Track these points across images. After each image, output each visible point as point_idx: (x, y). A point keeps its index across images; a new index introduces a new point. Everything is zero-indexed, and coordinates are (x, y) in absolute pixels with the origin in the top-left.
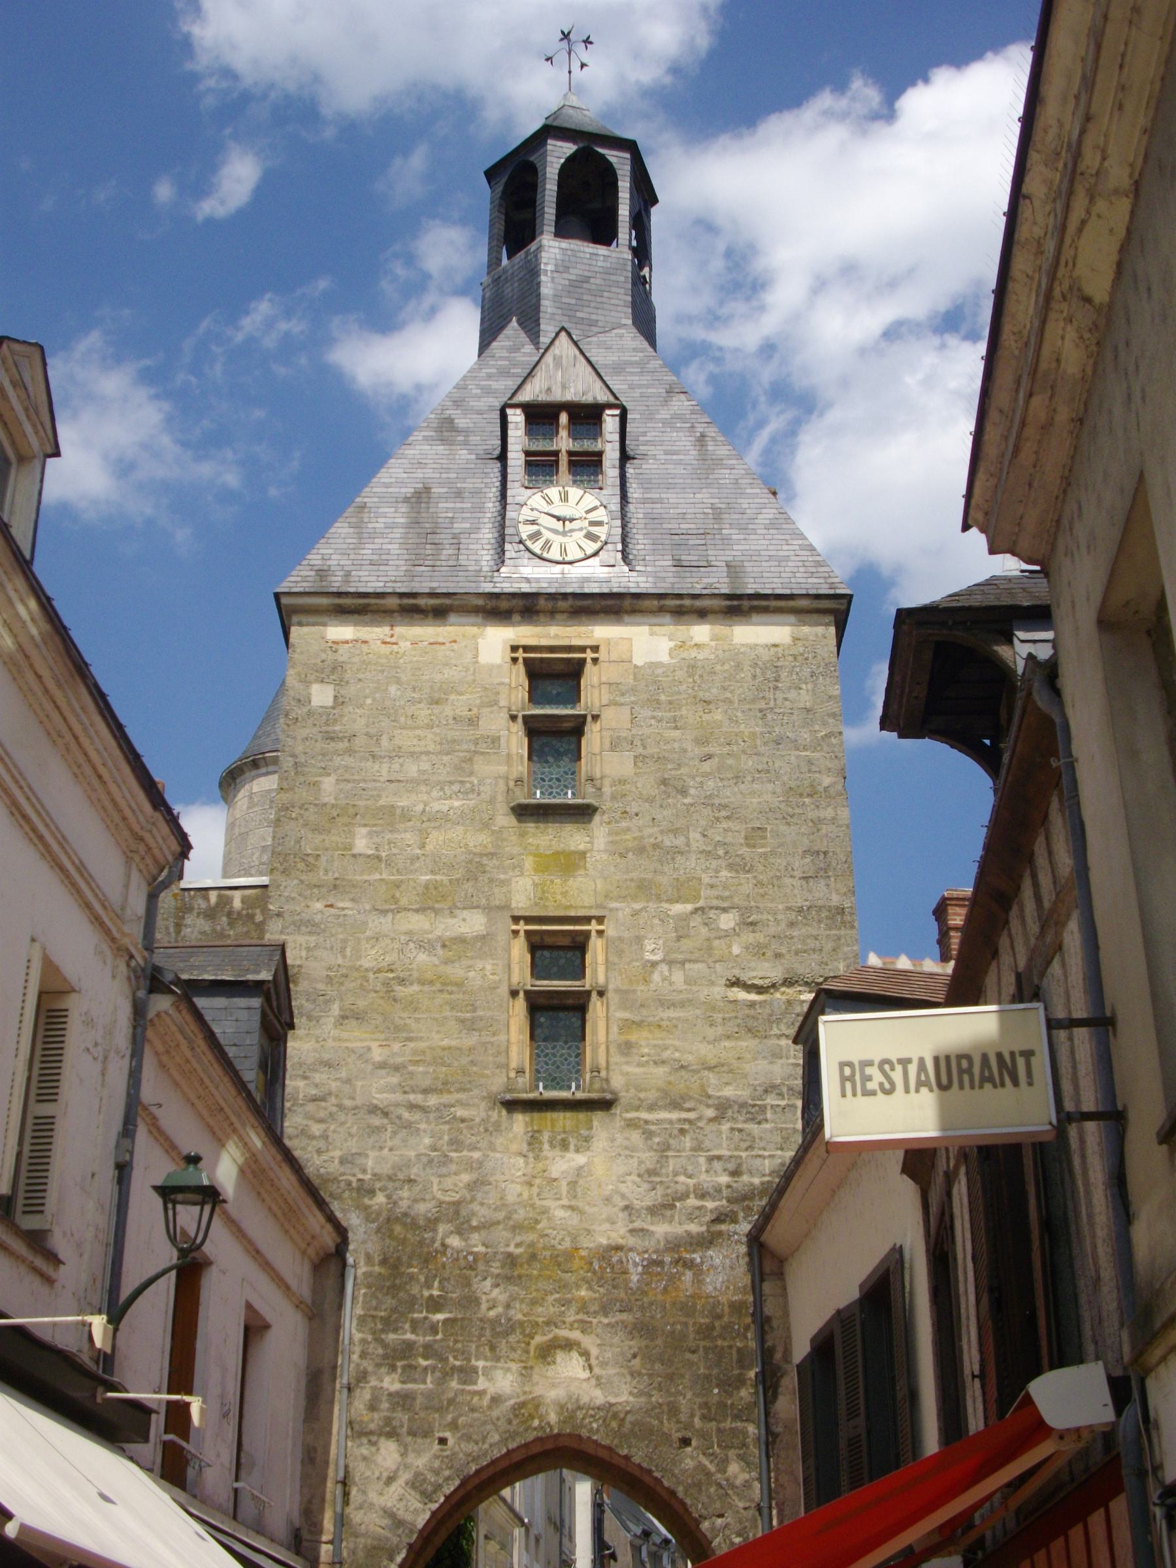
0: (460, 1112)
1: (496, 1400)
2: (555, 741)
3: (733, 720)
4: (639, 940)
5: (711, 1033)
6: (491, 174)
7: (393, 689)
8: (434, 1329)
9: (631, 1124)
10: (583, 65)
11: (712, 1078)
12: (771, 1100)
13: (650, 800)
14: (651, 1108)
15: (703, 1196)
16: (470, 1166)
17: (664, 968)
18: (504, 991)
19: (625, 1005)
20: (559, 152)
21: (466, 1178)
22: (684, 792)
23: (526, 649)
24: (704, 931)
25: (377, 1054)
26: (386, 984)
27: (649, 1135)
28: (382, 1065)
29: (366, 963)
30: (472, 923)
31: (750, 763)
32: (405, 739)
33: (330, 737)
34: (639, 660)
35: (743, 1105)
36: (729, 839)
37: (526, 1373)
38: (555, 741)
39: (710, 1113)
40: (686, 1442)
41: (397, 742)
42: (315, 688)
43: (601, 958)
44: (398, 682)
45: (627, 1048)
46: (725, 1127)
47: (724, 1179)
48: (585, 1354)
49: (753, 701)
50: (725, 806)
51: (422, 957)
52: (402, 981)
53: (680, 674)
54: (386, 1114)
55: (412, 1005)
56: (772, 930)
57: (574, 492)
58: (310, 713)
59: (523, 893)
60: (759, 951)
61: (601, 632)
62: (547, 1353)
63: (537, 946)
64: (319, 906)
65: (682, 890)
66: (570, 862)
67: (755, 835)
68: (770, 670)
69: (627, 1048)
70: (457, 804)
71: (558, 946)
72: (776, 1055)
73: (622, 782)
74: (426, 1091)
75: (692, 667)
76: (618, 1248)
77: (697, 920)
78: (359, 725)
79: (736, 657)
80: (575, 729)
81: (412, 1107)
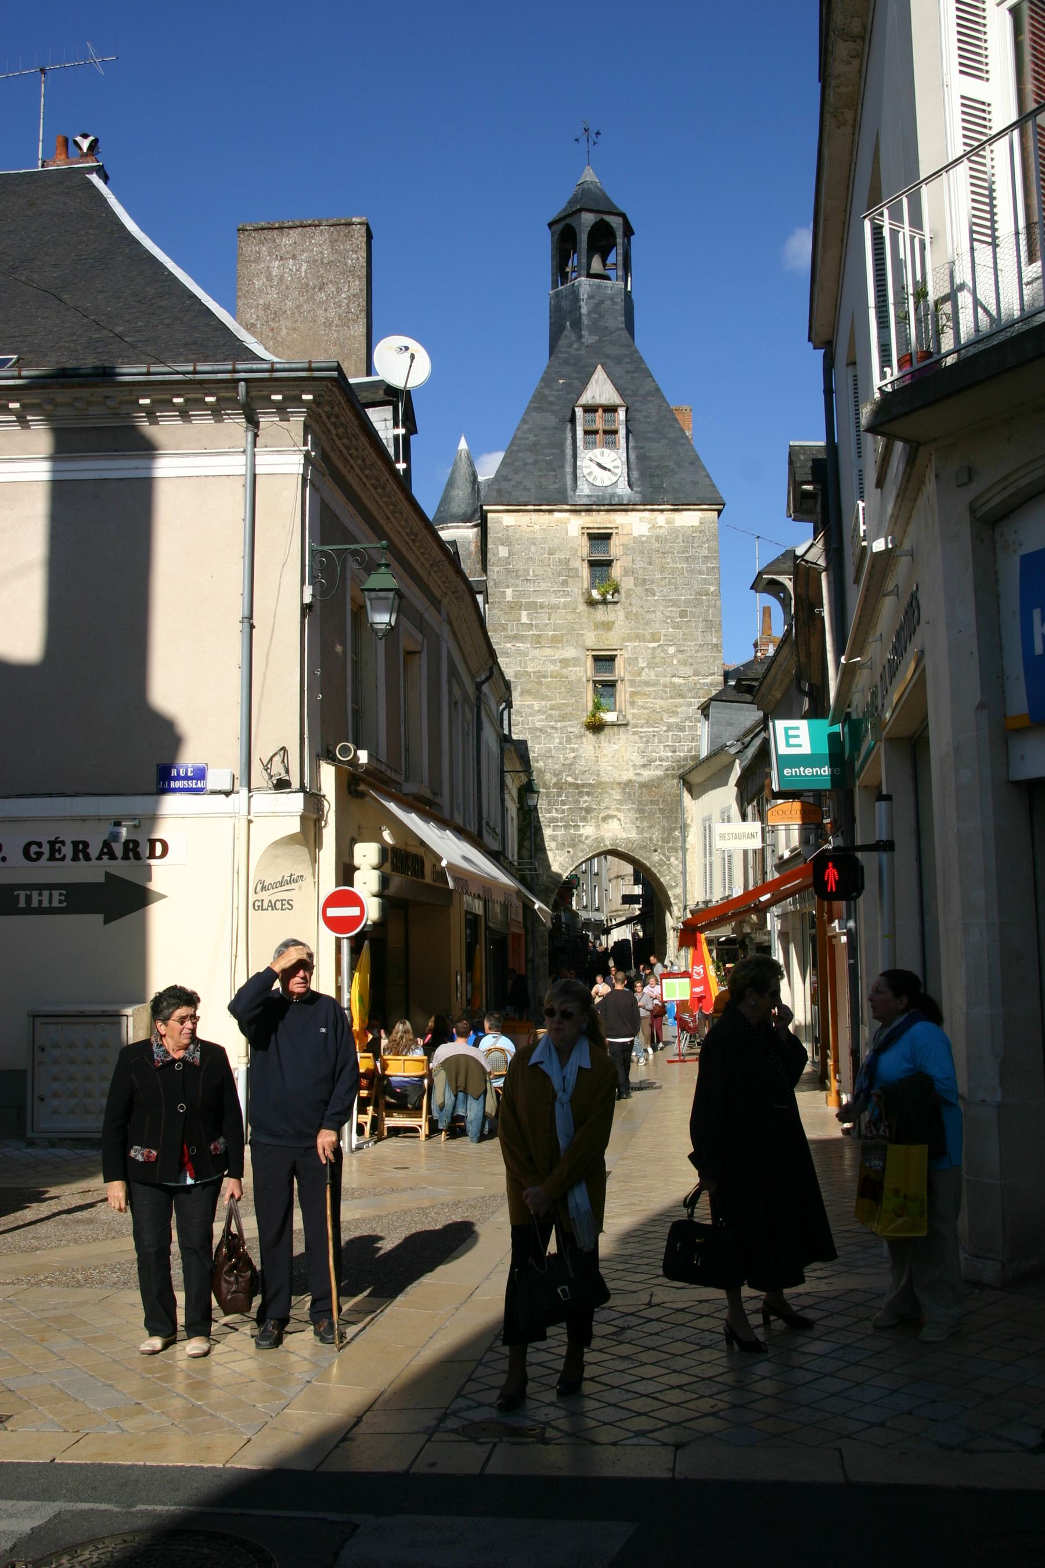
0: (570, 730)
1: (587, 838)
2: (600, 566)
3: (674, 562)
4: (636, 658)
5: (664, 695)
6: (550, 225)
7: (533, 548)
8: (563, 812)
9: (635, 733)
10: (595, 143)
11: (665, 715)
12: (687, 723)
13: (641, 598)
14: (642, 727)
15: (661, 760)
16: (573, 750)
17: (646, 670)
18: (584, 679)
19: (631, 687)
20: (588, 219)
21: (572, 755)
22: (654, 595)
23: (588, 528)
24: (662, 655)
25: (536, 708)
26: (538, 677)
27: (641, 737)
28: (538, 711)
29: (529, 669)
30: (570, 652)
31: (680, 581)
32: (540, 571)
33: (509, 571)
34: (635, 534)
35: (677, 725)
36: (673, 614)
37: (598, 826)
38: (600, 566)
39: (665, 728)
40: (656, 851)
41: (537, 573)
42: (500, 548)
43: (622, 666)
44: (535, 544)
45: (633, 704)
46: (670, 734)
47: (670, 754)
48: (619, 820)
49: (683, 552)
50: (671, 600)
51: (552, 667)
52: (545, 677)
53: (653, 540)
54: (541, 730)
55: (548, 686)
56: (689, 654)
57: (606, 451)
58: (499, 560)
59: (590, 638)
60: (684, 663)
61: (619, 519)
62: (605, 819)
63: (597, 659)
64: (509, 645)
65: (654, 638)
66: (608, 626)
67: (683, 614)
68: (689, 538)
69: (633, 704)
70: (562, 600)
71: (604, 661)
72: (690, 705)
73: (629, 590)
74: (556, 721)
75: (658, 538)
76: (630, 781)
77: (660, 649)
78: (521, 566)
79: (675, 532)
80: (609, 563)
81: (553, 728)
